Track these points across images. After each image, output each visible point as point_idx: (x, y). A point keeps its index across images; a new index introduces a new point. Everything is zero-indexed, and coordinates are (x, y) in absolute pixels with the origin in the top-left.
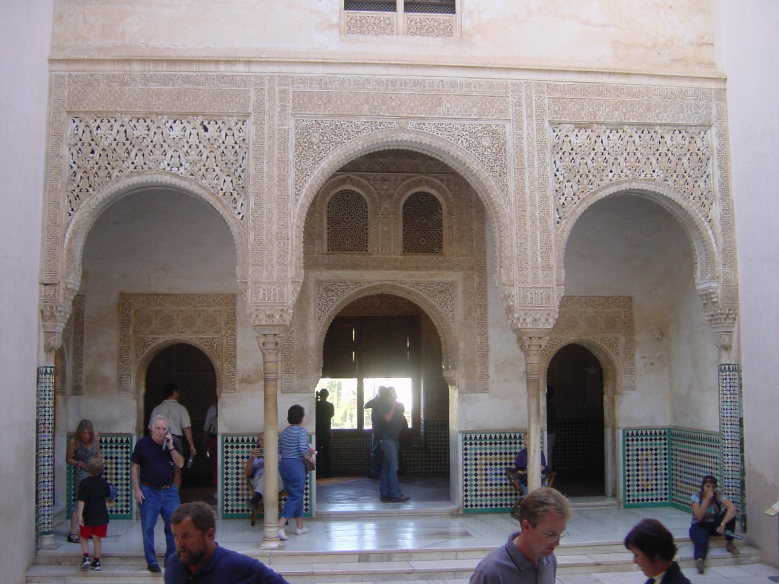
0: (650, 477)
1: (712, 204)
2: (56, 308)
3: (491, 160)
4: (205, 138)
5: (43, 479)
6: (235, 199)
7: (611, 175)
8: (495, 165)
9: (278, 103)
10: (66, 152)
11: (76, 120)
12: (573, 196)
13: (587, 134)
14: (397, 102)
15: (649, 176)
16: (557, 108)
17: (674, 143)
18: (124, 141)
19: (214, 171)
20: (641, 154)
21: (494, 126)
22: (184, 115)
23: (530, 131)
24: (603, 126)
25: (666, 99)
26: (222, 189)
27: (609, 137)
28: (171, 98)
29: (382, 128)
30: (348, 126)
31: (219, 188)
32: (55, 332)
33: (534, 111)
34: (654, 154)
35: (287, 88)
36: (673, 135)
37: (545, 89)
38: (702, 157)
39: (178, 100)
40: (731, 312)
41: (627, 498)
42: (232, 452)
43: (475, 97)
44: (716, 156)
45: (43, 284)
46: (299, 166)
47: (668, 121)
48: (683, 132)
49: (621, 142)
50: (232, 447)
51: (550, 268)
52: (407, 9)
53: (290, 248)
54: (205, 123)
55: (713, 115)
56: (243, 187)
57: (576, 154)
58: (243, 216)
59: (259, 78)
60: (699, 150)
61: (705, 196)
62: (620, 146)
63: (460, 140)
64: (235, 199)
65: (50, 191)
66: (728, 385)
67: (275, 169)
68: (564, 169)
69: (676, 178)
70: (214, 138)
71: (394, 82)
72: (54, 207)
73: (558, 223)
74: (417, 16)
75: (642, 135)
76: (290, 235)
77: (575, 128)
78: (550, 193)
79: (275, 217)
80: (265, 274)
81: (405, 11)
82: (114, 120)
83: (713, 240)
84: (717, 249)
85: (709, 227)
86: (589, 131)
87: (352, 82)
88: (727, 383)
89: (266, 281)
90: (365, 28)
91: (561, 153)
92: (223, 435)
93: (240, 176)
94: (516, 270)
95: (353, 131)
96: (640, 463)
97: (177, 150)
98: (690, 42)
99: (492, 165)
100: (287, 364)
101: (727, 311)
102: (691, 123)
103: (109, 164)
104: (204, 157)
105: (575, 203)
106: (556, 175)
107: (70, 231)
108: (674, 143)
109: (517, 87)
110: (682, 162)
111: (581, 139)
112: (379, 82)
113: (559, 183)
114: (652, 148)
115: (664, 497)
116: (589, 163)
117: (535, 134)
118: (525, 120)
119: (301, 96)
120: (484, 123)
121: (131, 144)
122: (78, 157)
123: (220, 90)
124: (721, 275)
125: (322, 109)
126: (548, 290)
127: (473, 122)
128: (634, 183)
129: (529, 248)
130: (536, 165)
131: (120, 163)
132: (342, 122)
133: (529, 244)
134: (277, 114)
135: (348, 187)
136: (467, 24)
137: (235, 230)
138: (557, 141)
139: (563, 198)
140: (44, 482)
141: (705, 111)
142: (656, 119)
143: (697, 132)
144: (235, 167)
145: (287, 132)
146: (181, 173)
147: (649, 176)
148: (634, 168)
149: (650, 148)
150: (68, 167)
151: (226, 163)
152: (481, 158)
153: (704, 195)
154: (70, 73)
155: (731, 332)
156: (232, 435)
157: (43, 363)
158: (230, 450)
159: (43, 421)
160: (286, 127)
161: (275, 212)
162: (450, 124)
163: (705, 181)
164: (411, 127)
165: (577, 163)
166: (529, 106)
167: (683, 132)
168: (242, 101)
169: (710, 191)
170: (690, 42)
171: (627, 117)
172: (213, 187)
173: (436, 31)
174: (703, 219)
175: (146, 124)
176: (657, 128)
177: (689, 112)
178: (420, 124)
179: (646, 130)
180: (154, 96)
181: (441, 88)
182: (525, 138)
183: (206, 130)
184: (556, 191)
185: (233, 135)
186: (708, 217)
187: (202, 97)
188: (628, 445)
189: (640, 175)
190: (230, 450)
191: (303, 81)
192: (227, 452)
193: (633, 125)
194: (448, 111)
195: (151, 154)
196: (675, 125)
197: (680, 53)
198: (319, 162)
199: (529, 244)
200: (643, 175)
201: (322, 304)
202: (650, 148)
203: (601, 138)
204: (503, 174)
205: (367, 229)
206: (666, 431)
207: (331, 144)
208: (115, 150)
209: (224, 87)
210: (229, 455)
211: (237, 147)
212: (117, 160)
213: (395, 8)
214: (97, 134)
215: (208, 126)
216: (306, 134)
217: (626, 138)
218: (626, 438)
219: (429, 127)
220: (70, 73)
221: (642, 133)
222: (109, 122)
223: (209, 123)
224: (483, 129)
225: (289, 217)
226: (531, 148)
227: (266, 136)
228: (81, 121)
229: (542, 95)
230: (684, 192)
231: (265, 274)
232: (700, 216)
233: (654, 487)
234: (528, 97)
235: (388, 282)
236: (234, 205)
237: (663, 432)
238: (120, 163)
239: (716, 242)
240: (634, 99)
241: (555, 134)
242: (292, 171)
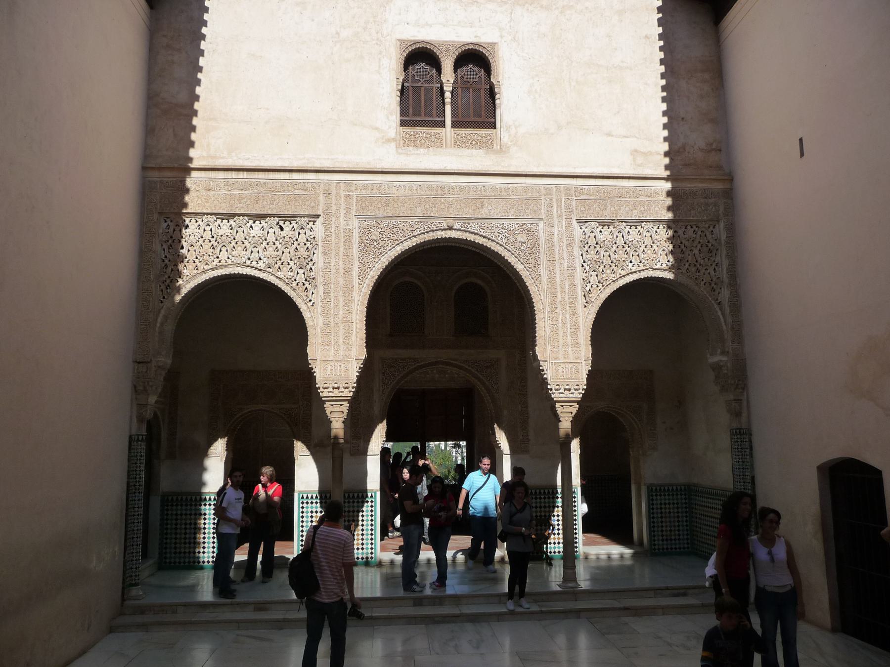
0: (673, 528)
1: (721, 289)
2: (148, 384)
3: (526, 254)
4: (281, 236)
5: (132, 536)
6: (306, 288)
7: (630, 265)
8: (530, 258)
9: (343, 206)
10: (157, 247)
11: (167, 220)
12: (598, 284)
13: (610, 230)
14: (446, 205)
16: (583, 209)
17: (686, 236)
18: (210, 239)
19: (289, 264)
20: (657, 246)
21: (529, 225)
22: (262, 217)
26: (295, 280)
27: (629, 232)
28: (251, 202)
29: (433, 228)
30: (404, 226)
31: (293, 279)
32: (147, 404)
33: (563, 211)
35: (351, 193)
36: (685, 230)
37: (573, 192)
39: (257, 203)
40: (740, 382)
41: (653, 547)
42: (307, 508)
43: (512, 200)
44: (724, 247)
45: (136, 362)
46: (362, 260)
47: (681, 218)
49: (640, 237)
50: (307, 503)
51: (578, 345)
52: (455, 125)
53: (354, 330)
54: (281, 223)
56: (314, 279)
57: (600, 247)
58: (314, 303)
59: (327, 185)
60: (708, 242)
62: (639, 240)
63: (500, 237)
64: (306, 288)
65: (144, 281)
66: (739, 447)
67: (341, 263)
68: (589, 260)
70: (289, 236)
71: (442, 188)
72: (148, 295)
73: (585, 307)
74: (463, 132)
75: (658, 230)
76: (354, 318)
78: (579, 282)
79: (341, 304)
80: (332, 353)
81: (452, 127)
82: (201, 220)
83: (722, 320)
84: (726, 327)
85: (718, 308)
87: (407, 188)
88: (738, 445)
89: (333, 359)
90: (418, 141)
91: (587, 247)
92: (300, 492)
93: (311, 269)
94: (548, 346)
95: (408, 230)
96: (664, 515)
97: (257, 246)
98: (700, 149)
99: (527, 258)
100: (355, 430)
101: (737, 381)
103: (197, 258)
104: (280, 253)
105: (600, 290)
106: (583, 266)
107: (161, 316)
108: (686, 236)
109: (548, 191)
111: (605, 234)
112: (430, 188)
115: (686, 546)
116: (612, 255)
118: (555, 219)
119: (364, 200)
120: (521, 222)
121: (216, 241)
122: (169, 252)
123: (293, 195)
124: (731, 351)
125: (381, 211)
126: (577, 365)
127: (511, 222)
129: (560, 329)
130: (565, 258)
131: (206, 257)
132: (399, 223)
133: (560, 325)
134: (342, 216)
135: (408, 279)
136: (506, 138)
137: (307, 315)
138: (584, 237)
140: (133, 538)
141: (714, 208)
143: (707, 226)
144: (307, 261)
145: (351, 231)
146: (260, 267)
150: (160, 261)
151: (299, 258)
152: (518, 252)
153: (714, 280)
154: (162, 179)
155: (741, 400)
156: (307, 492)
157: (134, 432)
158: (305, 505)
159: (134, 483)
160: (351, 227)
161: (341, 299)
162: (491, 223)
163: (715, 269)
164: (458, 226)
166: (559, 206)
168: (313, 204)
169: (719, 278)
170: (700, 149)
171: (644, 215)
172: (287, 278)
173: (479, 144)
174: (713, 302)
175: (230, 224)
177: (700, 209)
178: (465, 223)
179: (661, 225)
180: (236, 200)
181: (483, 193)
182: (556, 235)
183: (282, 229)
184: (583, 279)
185: (305, 234)
187: (277, 201)
188: (652, 500)
190: (305, 505)
191: (365, 187)
192: (303, 508)
194: (490, 212)
195: (233, 249)
197: (691, 158)
198: (378, 257)
199: (560, 325)
201: (386, 378)
204: (537, 265)
205: (423, 314)
206: (686, 488)
207: (389, 241)
208: (202, 246)
209: (297, 192)
210: (305, 510)
211: (308, 244)
212: (204, 255)
213: (444, 125)
214: (186, 232)
215: (283, 226)
216: (368, 232)
218: (651, 494)
219: (473, 226)
220: (162, 179)
222: (197, 222)
223: (284, 224)
224: (519, 228)
225: (354, 304)
227: (333, 235)
228: (171, 221)
229: (570, 198)
230: (696, 278)
231: (332, 353)
232: (710, 299)
233: (677, 537)
234: (559, 200)
235: (442, 359)
236: (306, 294)
237: (683, 488)
238: (206, 257)
239: (725, 322)
240: (650, 199)
242: (357, 264)
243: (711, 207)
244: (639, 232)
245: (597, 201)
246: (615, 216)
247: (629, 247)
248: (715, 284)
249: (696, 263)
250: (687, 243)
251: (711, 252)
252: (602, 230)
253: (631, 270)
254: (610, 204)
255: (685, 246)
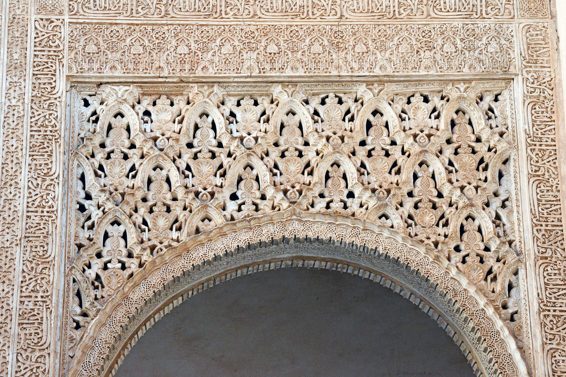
1: (516, 273)
7: (232, 206)
12: (125, 259)
15: (336, 206)
16: (91, 48)
17: (406, 124)
20: (318, 154)
23: (14, 102)
24: (216, 88)
25: (385, 20)
33: (30, 53)
34: (354, 153)
36: (406, 107)
38: (487, 156)
47: (389, 71)
48: (436, 101)
49: (263, 126)
55: (517, 51)
57: (142, 157)
61: (496, 252)
69: (412, 211)
73: (78, 327)
75: (321, 110)
77: (143, 94)
85: (507, 332)
86: (180, 103)
91: (100, 156)
102: (453, 74)
105: (131, 275)
106: (82, 208)
110: (431, 170)
113: (91, 227)
114: (346, 139)
117: (27, 107)
128: (296, 225)
138: (91, 126)
139: (97, 264)
141: (494, 43)
142: (356, 66)
143: (473, 95)
147: (336, 206)
148: (298, 187)
149: (342, 138)
153: (493, 249)
163: (498, 217)
165: (139, 181)
167: (436, 101)
171: (277, 66)
174: (490, 311)
176: (361, 90)
179: (331, 95)
184: (80, 246)
186: (505, 307)
189: (312, 206)
193: (295, 84)
196: (407, 81)
200: (321, 205)
202: (342, 138)
203: (210, 119)
217: (278, 116)
221: (323, 102)
226: (13, 142)
229: (53, 18)
230: (436, 244)
240: (298, 20)
241: (90, 110)
243: (484, 40)
244: (264, 113)
245: (137, 28)
246: (187, 67)
247: (230, 155)
248: (498, 260)
249: (436, 200)
250: (409, 142)
251: (485, 169)
252: (151, 109)
253: (232, 219)
254: (176, 35)
255: (403, 153)
